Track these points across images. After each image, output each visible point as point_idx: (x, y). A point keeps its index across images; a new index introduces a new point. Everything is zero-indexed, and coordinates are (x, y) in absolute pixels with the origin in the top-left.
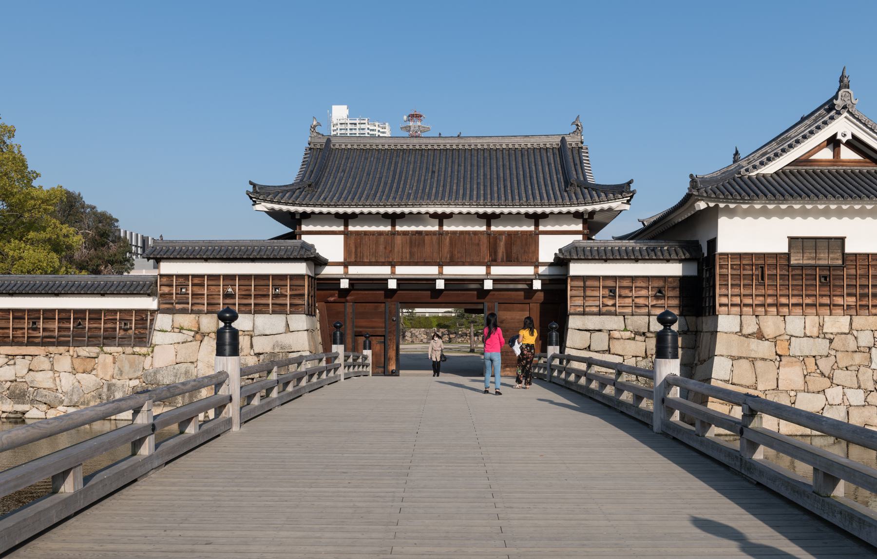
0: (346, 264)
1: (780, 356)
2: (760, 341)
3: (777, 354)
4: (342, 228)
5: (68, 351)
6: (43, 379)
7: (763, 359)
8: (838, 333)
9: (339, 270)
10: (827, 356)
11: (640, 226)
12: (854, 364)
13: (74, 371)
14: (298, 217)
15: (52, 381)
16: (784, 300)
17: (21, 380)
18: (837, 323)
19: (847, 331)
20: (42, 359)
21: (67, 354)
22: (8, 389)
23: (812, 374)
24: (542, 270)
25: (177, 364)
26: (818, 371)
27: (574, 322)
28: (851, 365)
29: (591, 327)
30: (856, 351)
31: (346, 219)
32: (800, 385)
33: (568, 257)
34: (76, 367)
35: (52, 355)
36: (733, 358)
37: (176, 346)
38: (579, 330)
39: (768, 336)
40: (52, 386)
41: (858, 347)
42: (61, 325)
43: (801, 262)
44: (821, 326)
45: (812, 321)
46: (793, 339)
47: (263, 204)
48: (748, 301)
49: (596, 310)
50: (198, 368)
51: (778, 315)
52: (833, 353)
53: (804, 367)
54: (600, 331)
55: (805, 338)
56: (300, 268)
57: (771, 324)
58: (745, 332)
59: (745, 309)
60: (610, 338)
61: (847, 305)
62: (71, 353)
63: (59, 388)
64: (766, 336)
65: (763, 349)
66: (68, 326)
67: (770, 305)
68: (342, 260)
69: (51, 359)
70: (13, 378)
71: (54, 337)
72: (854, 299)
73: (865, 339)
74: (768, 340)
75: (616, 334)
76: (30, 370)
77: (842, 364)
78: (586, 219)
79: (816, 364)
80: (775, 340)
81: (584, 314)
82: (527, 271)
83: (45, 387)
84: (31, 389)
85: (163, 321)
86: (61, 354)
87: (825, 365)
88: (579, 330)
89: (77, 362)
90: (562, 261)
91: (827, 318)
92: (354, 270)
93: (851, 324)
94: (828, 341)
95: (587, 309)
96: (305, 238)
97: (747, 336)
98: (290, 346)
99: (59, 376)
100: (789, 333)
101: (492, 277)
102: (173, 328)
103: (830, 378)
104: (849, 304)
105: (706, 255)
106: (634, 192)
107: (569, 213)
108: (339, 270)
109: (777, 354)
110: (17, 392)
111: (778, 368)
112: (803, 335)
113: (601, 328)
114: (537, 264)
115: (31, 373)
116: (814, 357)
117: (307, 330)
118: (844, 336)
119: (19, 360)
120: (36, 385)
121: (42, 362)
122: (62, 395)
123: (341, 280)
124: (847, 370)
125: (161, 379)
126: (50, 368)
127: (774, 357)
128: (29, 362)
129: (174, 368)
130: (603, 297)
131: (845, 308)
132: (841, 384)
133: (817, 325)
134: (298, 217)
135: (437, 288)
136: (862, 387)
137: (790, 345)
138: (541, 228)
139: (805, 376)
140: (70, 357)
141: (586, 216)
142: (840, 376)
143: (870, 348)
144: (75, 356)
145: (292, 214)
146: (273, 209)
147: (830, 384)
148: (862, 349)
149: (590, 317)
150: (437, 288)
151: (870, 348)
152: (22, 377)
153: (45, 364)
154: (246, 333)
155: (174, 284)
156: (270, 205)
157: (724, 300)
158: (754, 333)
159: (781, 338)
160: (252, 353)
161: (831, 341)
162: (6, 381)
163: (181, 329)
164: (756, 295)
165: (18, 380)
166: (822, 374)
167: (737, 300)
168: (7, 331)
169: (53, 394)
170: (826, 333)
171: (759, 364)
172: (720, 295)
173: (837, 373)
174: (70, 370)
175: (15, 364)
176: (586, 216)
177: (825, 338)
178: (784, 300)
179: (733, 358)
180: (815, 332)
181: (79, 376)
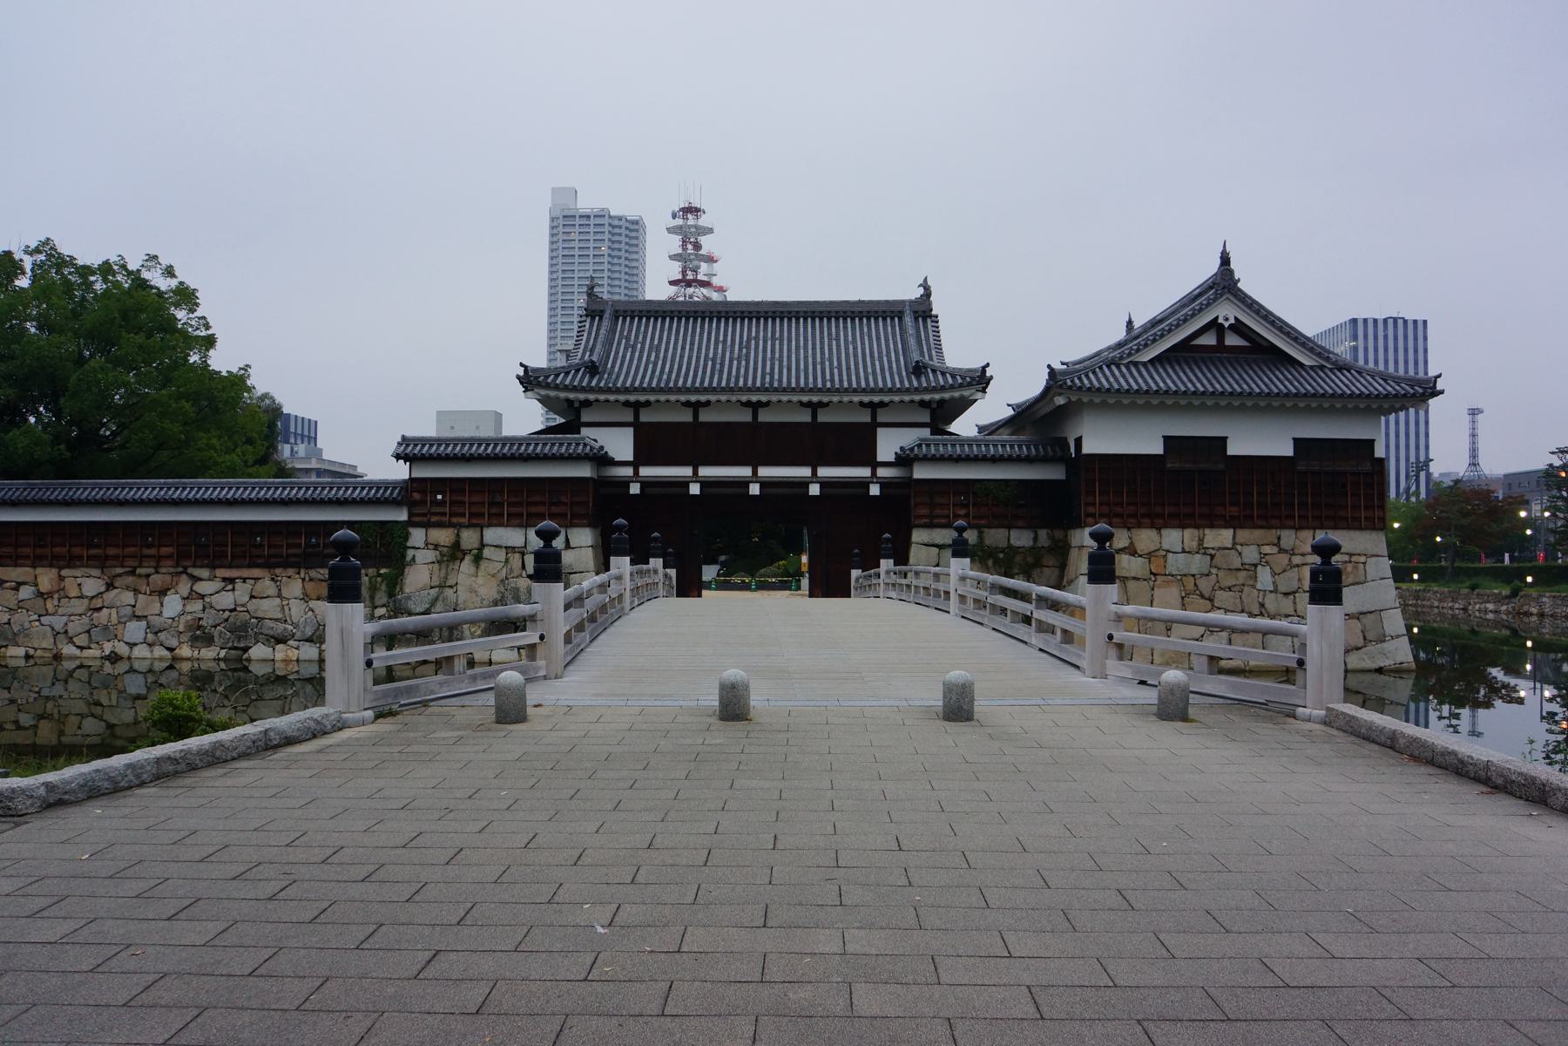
1: (1155, 575)
2: (1132, 557)
4: (630, 419)
5: (299, 573)
6: (269, 607)
7: (1134, 578)
8: (1220, 548)
9: (629, 471)
11: (1010, 412)
12: (1238, 583)
13: (306, 597)
14: (577, 405)
15: (279, 609)
16: (1158, 509)
17: (242, 609)
18: (1220, 537)
19: (1230, 546)
20: (268, 582)
21: (297, 576)
22: (227, 620)
23: (1191, 596)
24: (882, 472)
25: (432, 588)
26: (1198, 592)
27: (918, 536)
28: (1235, 585)
29: (939, 541)
31: (637, 407)
33: (912, 456)
34: (308, 592)
35: (279, 578)
37: (430, 566)
39: (1142, 550)
40: (280, 616)
41: (1242, 564)
42: (290, 541)
43: (1177, 465)
44: (1201, 541)
45: (1190, 536)
46: (1170, 555)
47: (536, 390)
48: (1118, 510)
49: (943, 521)
50: (458, 592)
52: (1214, 571)
53: (1182, 588)
55: (1183, 555)
56: (584, 471)
59: (1115, 520)
61: (1230, 516)
62: (302, 576)
63: (288, 619)
64: (1139, 552)
66: (297, 541)
67: (1144, 516)
68: (630, 458)
69: (278, 583)
70: (232, 607)
71: (281, 556)
72: (1236, 509)
73: (1250, 554)
74: (1140, 556)
76: (252, 597)
78: (934, 409)
79: (1195, 584)
80: (1150, 556)
81: (930, 526)
82: (864, 472)
83: (272, 617)
84: (252, 620)
85: (417, 536)
86: (289, 577)
87: (1205, 585)
89: (309, 586)
90: (904, 460)
91: (1207, 531)
92: (646, 471)
93: (1234, 537)
94: (1209, 558)
95: (935, 521)
96: (585, 431)
98: (570, 565)
99: (288, 604)
100: (1166, 546)
101: (819, 479)
102: (427, 545)
103: (1211, 600)
104: (1232, 514)
105: (1073, 456)
106: (991, 378)
107: (912, 401)
108: (629, 471)
109: (1151, 573)
110: (238, 623)
111: (1153, 589)
112: (1180, 551)
114: (874, 464)
115: (254, 600)
116: (1193, 576)
117: (591, 546)
118: (1227, 551)
119: (239, 584)
120: (261, 615)
121: (267, 586)
122: (292, 627)
123: (631, 484)
124: (1231, 590)
125: (413, 606)
126: (276, 594)
127: (1147, 575)
128: (251, 587)
129: (429, 594)
130: (954, 505)
131: (1227, 518)
132: (1224, 606)
133: (1197, 539)
134: (577, 405)
136: (1246, 609)
137: (1166, 562)
138: (880, 419)
139: (1183, 598)
140: (300, 580)
141: (934, 406)
143: (1255, 566)
144: (307, 579)
145: (569, 402)
146: (548, 397)
148: (1247, 567)
149: (938, 530)
150: (750, 493)
151: (1255, 566)
152: (243, 606)
153: (272, 591)
154: (517, 550)
155: (429, 490)
156: (543, 392)
157: (1091, 510)
158: (1125, 548)
159: (1157, 554)
160: (524, 574)
161: (1212, 557)
162: (224, 611)
163: (436, 547)
164: (1128, 504)
165: (238, 609)
167: (1105, 509)
168: (225, 549)
169: (281, 626)
170: (1208, 548)
172: (1087, 504)
173: (1219, 593)
174: (302, 597)
175: (233, 590)
176: (934, 406)
177: (1205, 554)
178: (1158, 509)
180: (1195, 544)
181: (313, 604)
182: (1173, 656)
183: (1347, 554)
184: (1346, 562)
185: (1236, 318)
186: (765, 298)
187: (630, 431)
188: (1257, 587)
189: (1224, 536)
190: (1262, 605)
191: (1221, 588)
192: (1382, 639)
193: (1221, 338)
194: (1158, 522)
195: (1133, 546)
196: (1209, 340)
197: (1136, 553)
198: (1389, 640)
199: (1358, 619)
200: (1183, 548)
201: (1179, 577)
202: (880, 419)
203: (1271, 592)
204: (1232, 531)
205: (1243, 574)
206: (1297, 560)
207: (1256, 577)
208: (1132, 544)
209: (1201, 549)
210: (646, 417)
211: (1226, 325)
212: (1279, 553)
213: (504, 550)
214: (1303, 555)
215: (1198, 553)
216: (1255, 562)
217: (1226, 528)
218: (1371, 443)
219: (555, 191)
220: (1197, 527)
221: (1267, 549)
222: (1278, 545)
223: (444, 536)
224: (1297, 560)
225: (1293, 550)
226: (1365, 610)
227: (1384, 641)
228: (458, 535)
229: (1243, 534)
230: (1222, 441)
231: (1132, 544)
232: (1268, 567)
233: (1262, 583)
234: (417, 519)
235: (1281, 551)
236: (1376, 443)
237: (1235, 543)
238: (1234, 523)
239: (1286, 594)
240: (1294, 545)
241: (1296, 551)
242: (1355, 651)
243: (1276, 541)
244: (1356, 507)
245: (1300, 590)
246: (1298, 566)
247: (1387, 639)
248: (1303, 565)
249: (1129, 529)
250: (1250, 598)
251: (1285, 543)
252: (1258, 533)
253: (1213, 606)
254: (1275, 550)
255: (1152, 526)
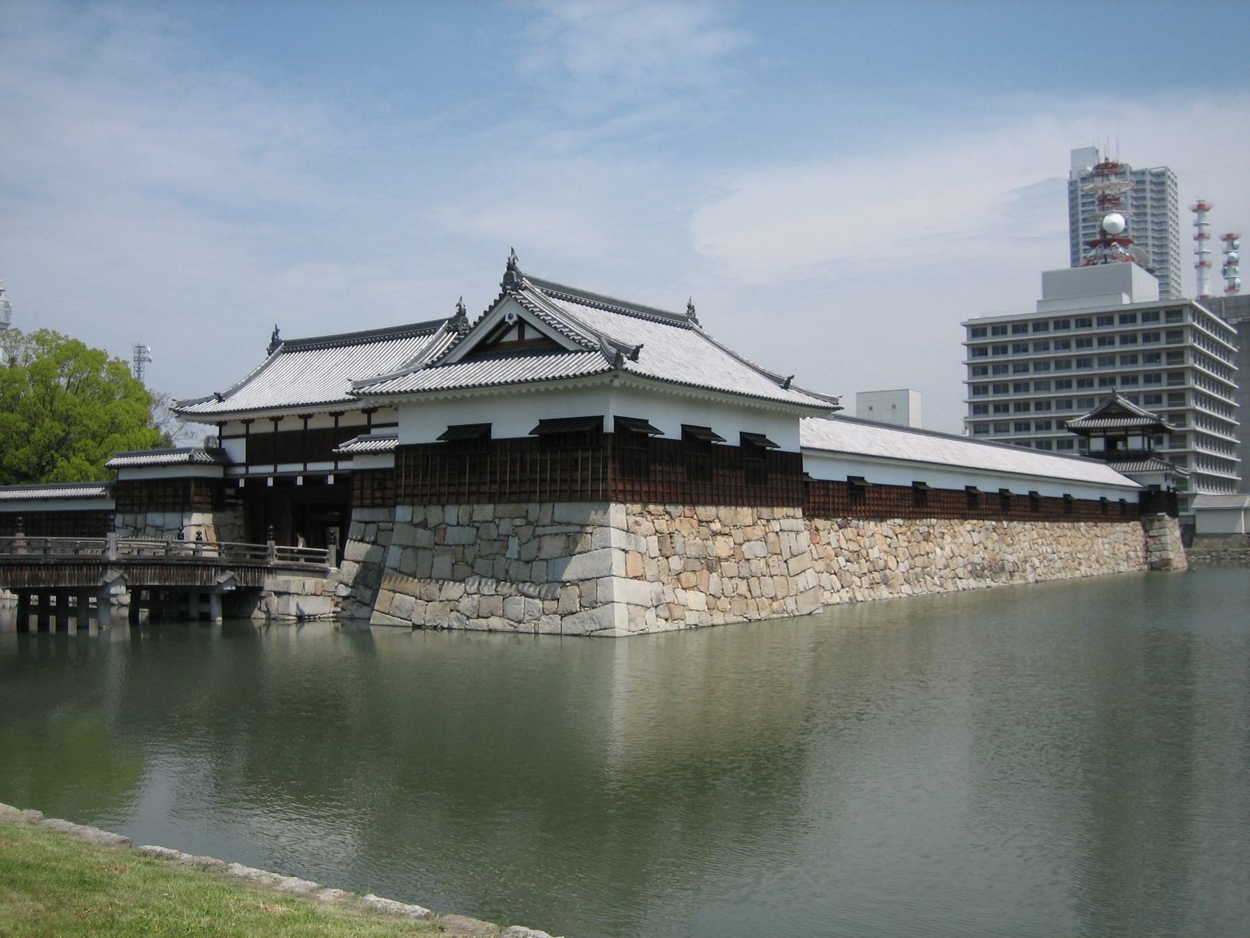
0: (247, 465)
3: (436, 544)
7: (425, 548)
8: (483, 522)
9: (242, 470)
10: (473, 545)
19: (490, 519)
27: (356, 514)
29: (367, 519)
30: (496, 540)
31: (247, 422)
32: (448, 574)
36: (404, 547)
38: (359, 522)
41: (498, 536)
44: (471, 515)
45: (464, 509)
46: (449, 528)
51: (420, 505)
52: (479, 541)
54: (374, 522)
55: (458, 528)
57: (434, 514)
58: (417, 520)
60: (378, 530)
65: (424, 537)
73: (505, 526)
74: (430, 529)
75: (382, 525)
77: (484, 553)
79: (464, 553)
80: (435, 529)
81: (362, 506)
85: (119, 519)
88: (359, 522)
92: (254, 470)
93: (495, 509)
94: (475, 530)
97: (416, 526)
100: (447, 520)
108: (242, 470)
111: (434, 557)
112: (456, 524)
113: (374, 520)
116: (464, 545)
118: (487, 524)
133: (468, 514)
135: (329, 483)
137: (445, 533)
138: (374, 422)
139: (453, 565)
142: (481, 564)
143: (508, 536)
147: (470, 572)
148: (502, 538)
151: (508, 536)
158: (421, 523)
159: (440, 527)
161: (478, 529)
166: (467, 563)
170: (475, 522)
171: (421, 553)
177: (473, 526)
179: (404, 547)
180: (464, 519)
182: (439, 614)
183: (578, 525)
184: (578, 533)
185: (519, 317)
186: (387, 327)
187: (245, 440)
188: (508, 555)
189: (485, 511)
190: (507, 572)
191: (481, 557)
192: (593, 605)
193: (521, 334)
194: (442, 500)
195: (427, 521)
196: (512, 336)
197: (427, 526)
198: (600, 606)
199: (578, 585)
200: (458, 522)
201: (453, 547)
202: (374, 422)
203: (516, 560)
204: (492, 506)
205: (498, 544)
206: (539, 531)
207: (508, 548)
208: (426, 519)
209: (471, 523)
210: (254, 429)
211: (511, 322)
212: (527, 524)
213: (155, 528)
214: (544, 526)
215: (468, 526)
216: (507, 533)
217: (489, 503)
218: (600, 419)
219: (1075, 154)
220: (468, 503)
221: (518, 522)
222: (525, 518)
223: (129, 518)
224: (539, 531)
225: (537, 521)
226: (583, 577)
227: (594, 608)
228: (136, 520)
229: (502, 509)
230: (487, 427)
231: (426, 519)
232: (517, 538)
233: (510, 554)
234: (119, 508)
235: (529, 523)
236: (604, 419)
237: (495, 517)
238: (491, 499)
239: (527, 562)
240: (538, 517)
241: (539, 523)
242: (571, 616)
243: (525, 515)
244: (584, 481)
245: (537, 559)
246: (539, 536)
247: (598, 605)
248: (544, 535)
249: (425, 506)
250: (501, 563)
251: (532, 517)
252: (512, 508)
253: (472, 571)
254: (523, 522)
255: (438, 503)
